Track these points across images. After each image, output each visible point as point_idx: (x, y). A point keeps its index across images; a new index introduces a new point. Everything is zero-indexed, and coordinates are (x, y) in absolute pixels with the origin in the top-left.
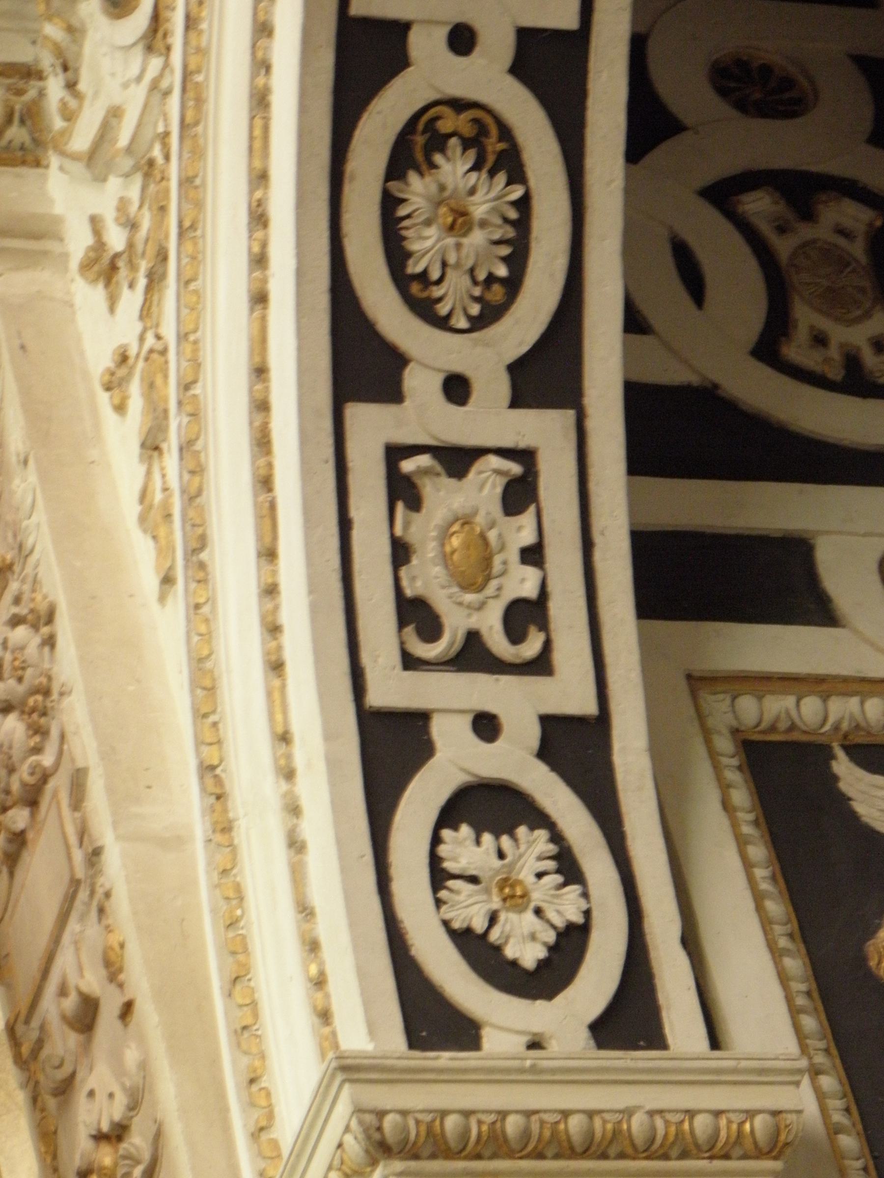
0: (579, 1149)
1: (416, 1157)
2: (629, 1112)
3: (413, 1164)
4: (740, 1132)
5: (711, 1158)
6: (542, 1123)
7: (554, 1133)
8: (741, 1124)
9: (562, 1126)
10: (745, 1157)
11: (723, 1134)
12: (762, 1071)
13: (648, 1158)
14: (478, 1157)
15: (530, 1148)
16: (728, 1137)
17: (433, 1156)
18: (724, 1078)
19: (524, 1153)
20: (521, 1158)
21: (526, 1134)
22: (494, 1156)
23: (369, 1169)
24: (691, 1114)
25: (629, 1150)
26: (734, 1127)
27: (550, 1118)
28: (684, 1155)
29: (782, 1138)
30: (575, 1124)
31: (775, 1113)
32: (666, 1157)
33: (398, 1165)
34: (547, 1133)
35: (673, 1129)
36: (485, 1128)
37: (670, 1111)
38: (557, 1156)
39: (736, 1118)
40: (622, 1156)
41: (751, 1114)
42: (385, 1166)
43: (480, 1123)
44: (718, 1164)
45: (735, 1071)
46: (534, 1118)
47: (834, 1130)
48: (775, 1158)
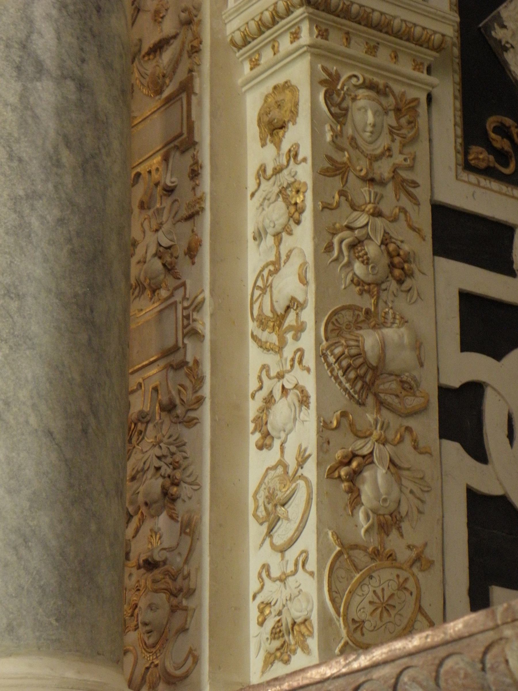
0: (374, 26)
1: (318, 9)
2: (395, 17)
3: (316, 11)
4: (429, 39)
5: (416, 44)
6: (365, 11)
7: (368, 17)
8: (431, 36)
9: (371, 15)
10: (428, 48)
11: (424, 37)
12: (444, 17)
13: (395, 37)
14: (338, 16)
15: (358, 19)
16: (425, 38)
17: (323, 11)
18: (431, 15)
19: (355, 20)
20: (353, 22)
21: (358, 14)
22: (345, 18)
23: (298, 7)
24: (415, 25)
25: (390, 32)
26: (428, 35)
27: (369, 10)
28: (408, 40)
29: (443, 45)
30: (376, 15)
31: (443, 35)
32: (401, 38)
33: (311, 10)
34: (365, 16)
35: (408, 29)
36: (345, 6)
37: (408, 22)
38: (365, 25)
39: (430, 32)
40: (387, 33)
41: (435, 32)
42: (306, 8)
43: (344, 3)
44: (418, 48)
45: (435, 14)
46: (362, 8)
47: (454, 44)
48: (437, 52)
